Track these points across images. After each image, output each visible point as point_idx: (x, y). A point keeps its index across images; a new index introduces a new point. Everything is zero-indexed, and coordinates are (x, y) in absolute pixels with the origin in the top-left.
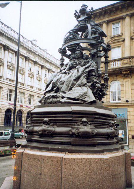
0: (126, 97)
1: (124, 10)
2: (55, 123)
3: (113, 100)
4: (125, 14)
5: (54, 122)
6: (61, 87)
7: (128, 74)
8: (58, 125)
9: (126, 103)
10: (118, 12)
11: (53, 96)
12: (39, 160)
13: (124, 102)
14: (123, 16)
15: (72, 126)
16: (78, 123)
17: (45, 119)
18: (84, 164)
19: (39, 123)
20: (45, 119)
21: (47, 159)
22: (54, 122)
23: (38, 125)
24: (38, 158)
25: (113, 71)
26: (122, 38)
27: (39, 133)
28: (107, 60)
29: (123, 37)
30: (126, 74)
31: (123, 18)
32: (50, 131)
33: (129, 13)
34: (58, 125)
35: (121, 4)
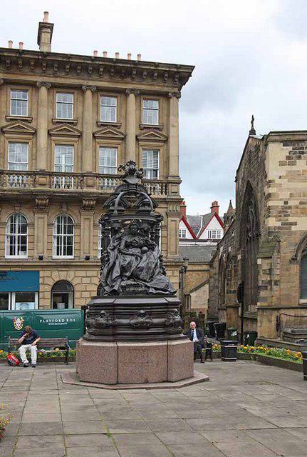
0: (37, 249)
1: (38, 71)
2: (150, 315)
3: (11, 254)
4: (39, 79)
7: (45, 205)
9: (38, 260)
10: (26, 70)
13: (35, 260)
14: (36, 82)
17: (142, 311)
20: (142, 311)
25: (20, 195)
26: (31, 127)
29: (33, 124)
30: (41, 205)
31: (34, 86)
32: (147, 323)
33: (46, 79)
35: (37, 57)
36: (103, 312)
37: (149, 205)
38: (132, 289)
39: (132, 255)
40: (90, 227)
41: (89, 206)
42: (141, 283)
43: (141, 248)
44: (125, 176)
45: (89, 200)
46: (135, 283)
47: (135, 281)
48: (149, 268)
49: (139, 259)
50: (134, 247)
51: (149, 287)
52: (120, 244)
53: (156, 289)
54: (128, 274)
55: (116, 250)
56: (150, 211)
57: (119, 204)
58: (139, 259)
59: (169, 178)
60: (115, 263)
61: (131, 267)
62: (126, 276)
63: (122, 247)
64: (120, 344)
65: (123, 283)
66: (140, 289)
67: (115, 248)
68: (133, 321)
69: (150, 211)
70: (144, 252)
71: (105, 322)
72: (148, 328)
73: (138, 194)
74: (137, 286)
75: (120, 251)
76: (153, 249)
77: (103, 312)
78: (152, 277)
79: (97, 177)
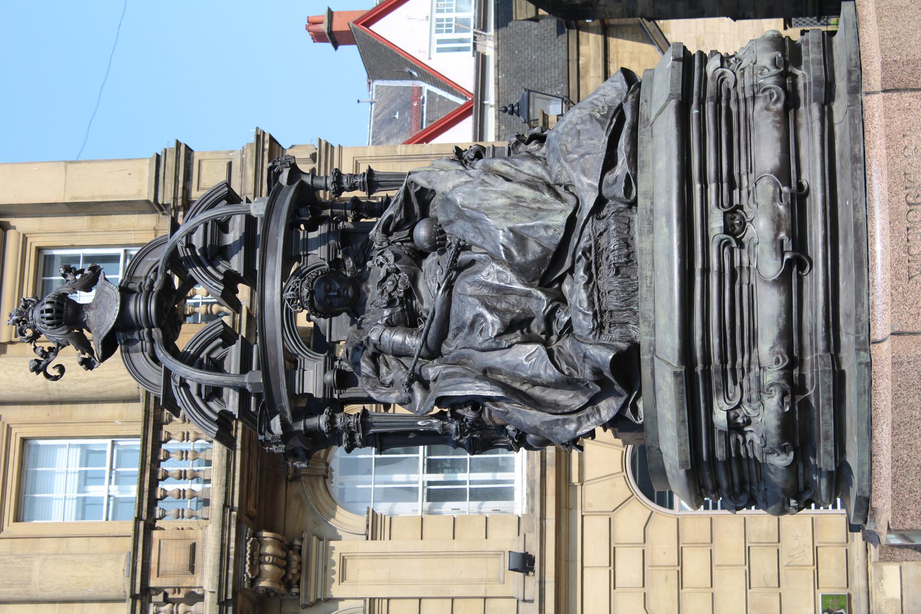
5: (732, 186)
6: (539, 249)
8: (743, 169)
11: (588, 269)
12: (910, 199)
15: (745, 100)
16: (731, 86)
18: (900, 20)
19: (737, 287)
20: (716, 223)
21: (902, 157)
22: (732, 186)
23: (745, 288)
24: (904, 207)
27: (787, 256)
28: (286, 460)
34: (743, 169)
36: (720, 418)
37: (222, 226)
38: (607, 280)
39: (449, 287)
40: (383, 556)
41: (283, 562)
42: (583, 241)
43: (419, 255)
44: (83, 345)
45: (257, 560)
46: (580, 273)
47: (571, 271)
48: (517, 203)
49: (464, 257)
50: (411, 292)
51: (601, 202)
52: (400, 353)
53: (610, 162)
54: (540, 302)
55: (432, 371)
56: (250, 221)
57: (217, 366)
58: (464, 257)
59: (166, 197)
60: (486, 374)
61: (503, 291)
62: (549, 318)
63: (413, 342)
64: (881, 329)
65: (584, 323)
66: (611, 243)
67: (416, 378)
68: (771, 267)
69: (250, 221)
70: (439, 242)
71: (772, 402)
72: (800, 197)
73: (168, 281)
74: (594, 254)
75: (433, 353)
76: (425, 196)
77: (720, 418)
78: (550, 188)
79: (150, 527)
